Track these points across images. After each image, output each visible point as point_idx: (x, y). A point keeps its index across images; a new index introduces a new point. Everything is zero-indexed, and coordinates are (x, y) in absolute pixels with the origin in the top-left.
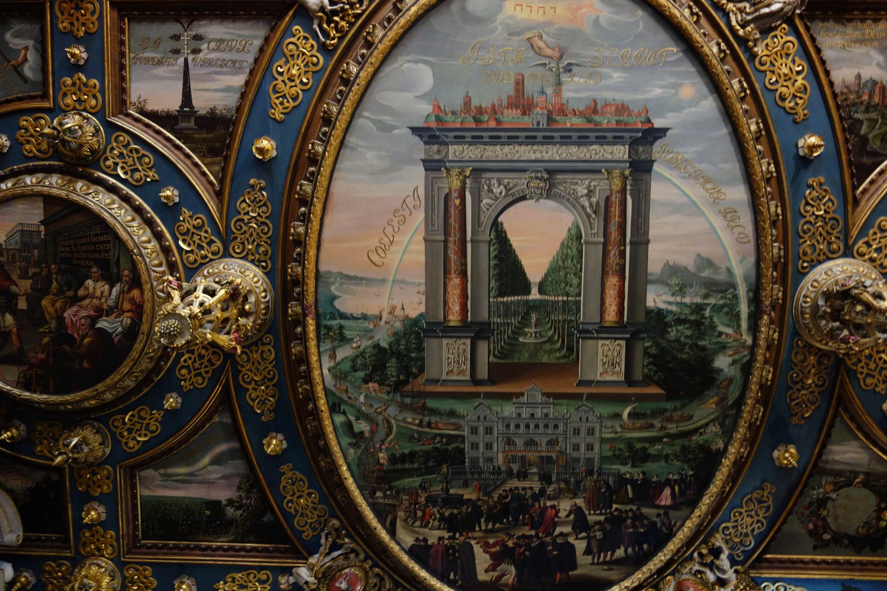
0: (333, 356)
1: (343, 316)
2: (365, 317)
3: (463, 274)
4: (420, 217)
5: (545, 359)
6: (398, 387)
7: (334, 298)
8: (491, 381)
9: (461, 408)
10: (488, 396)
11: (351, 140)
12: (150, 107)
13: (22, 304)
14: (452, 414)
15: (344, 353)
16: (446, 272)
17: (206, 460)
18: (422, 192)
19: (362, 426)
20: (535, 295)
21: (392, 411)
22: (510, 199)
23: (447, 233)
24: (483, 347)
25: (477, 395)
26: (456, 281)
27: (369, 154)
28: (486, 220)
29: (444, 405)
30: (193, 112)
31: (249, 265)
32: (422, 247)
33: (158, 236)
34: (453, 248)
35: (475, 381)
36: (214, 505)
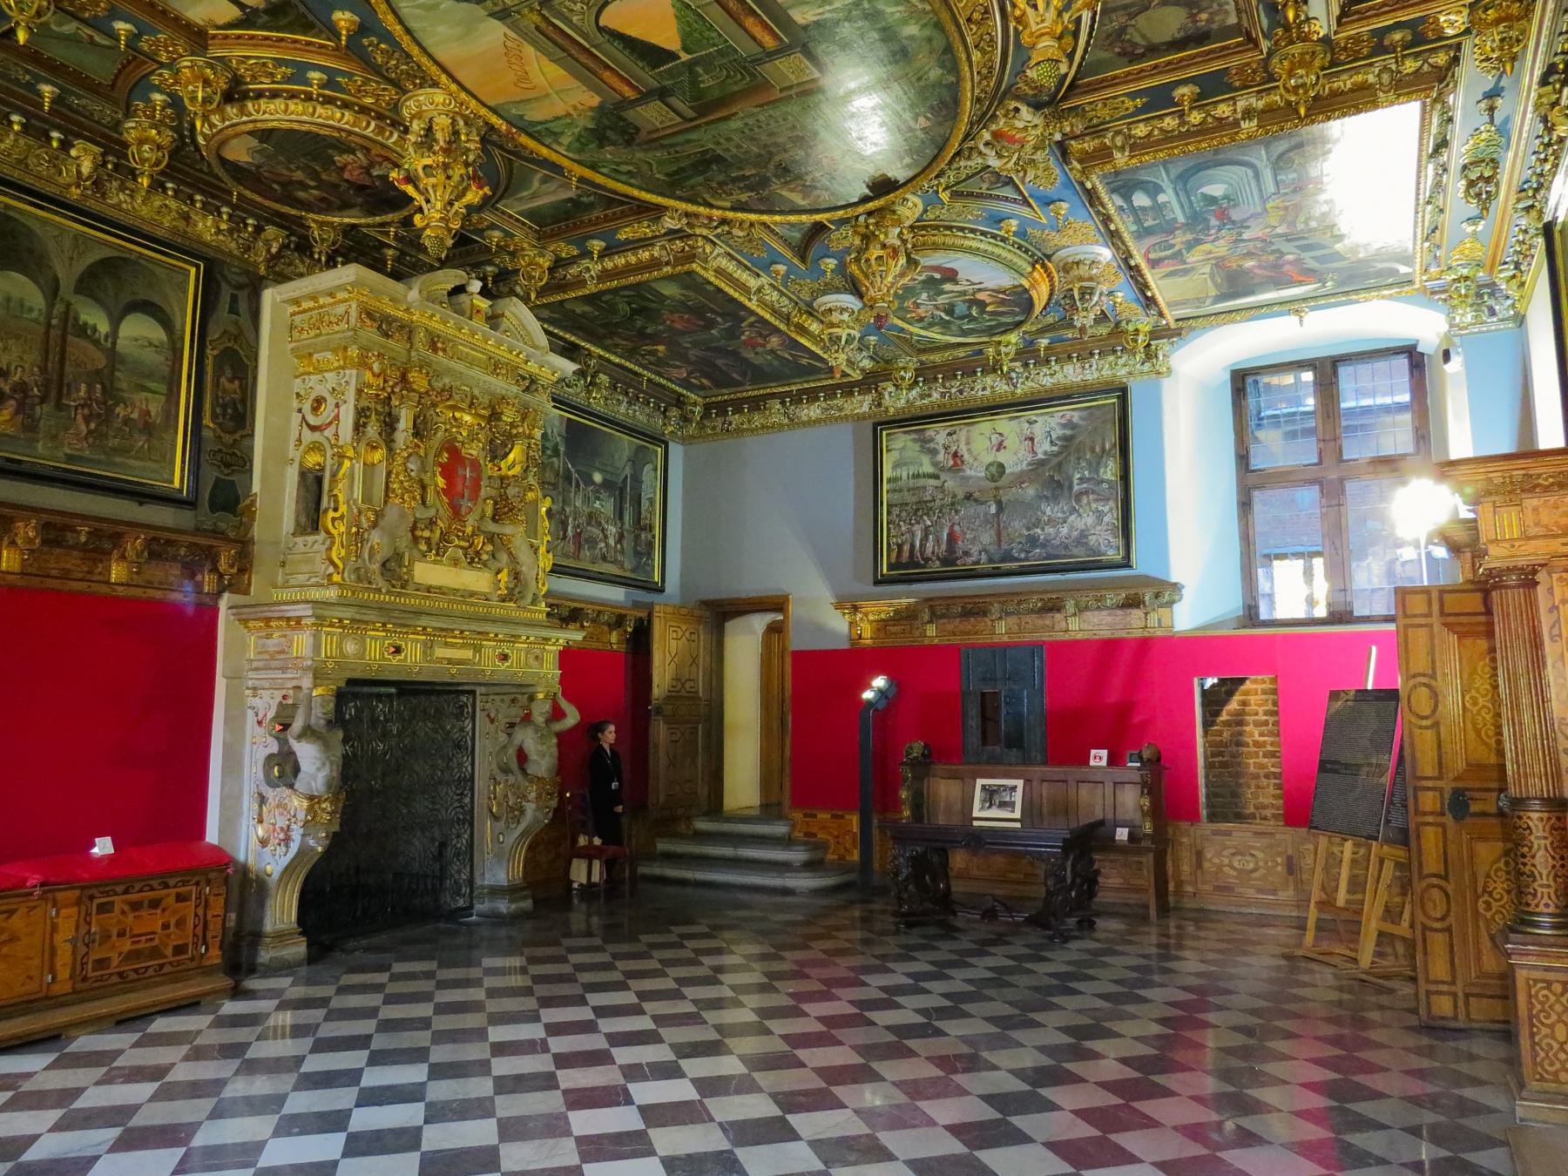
0: (560, 144)
1: (541, 123)
2: (557, 118)
3: (607, 67)
4: (529, 50)
5: (736, 88)
6: (629, 143)
7: (521, 117)
8: (701, 115)
9: (693, 136)
10: (707, 124)
11: (413, 25)
12: (221, 22)
13: (312, 183)
14: (688, 141)
15: (566, 140)
16: (594, 73)
17: (536, 184)
18: (512, 34)
19: (624, 168)
20: (685, 57)
21: (640, 155)
22: (595, 9)
23: (564, 50)
24: (673, 101)
25: (699, 126)
26: (607, 75)
27: (440, 29)
28: (589, 27)
29: (680, 139)
30: (255, 11)
31: (429, 90)
32: (554, 66)
33: (346, 105)
34: (583, 58)
35: (692, 120)
36: (570, 200)
